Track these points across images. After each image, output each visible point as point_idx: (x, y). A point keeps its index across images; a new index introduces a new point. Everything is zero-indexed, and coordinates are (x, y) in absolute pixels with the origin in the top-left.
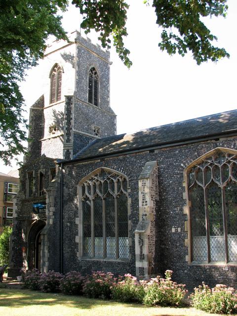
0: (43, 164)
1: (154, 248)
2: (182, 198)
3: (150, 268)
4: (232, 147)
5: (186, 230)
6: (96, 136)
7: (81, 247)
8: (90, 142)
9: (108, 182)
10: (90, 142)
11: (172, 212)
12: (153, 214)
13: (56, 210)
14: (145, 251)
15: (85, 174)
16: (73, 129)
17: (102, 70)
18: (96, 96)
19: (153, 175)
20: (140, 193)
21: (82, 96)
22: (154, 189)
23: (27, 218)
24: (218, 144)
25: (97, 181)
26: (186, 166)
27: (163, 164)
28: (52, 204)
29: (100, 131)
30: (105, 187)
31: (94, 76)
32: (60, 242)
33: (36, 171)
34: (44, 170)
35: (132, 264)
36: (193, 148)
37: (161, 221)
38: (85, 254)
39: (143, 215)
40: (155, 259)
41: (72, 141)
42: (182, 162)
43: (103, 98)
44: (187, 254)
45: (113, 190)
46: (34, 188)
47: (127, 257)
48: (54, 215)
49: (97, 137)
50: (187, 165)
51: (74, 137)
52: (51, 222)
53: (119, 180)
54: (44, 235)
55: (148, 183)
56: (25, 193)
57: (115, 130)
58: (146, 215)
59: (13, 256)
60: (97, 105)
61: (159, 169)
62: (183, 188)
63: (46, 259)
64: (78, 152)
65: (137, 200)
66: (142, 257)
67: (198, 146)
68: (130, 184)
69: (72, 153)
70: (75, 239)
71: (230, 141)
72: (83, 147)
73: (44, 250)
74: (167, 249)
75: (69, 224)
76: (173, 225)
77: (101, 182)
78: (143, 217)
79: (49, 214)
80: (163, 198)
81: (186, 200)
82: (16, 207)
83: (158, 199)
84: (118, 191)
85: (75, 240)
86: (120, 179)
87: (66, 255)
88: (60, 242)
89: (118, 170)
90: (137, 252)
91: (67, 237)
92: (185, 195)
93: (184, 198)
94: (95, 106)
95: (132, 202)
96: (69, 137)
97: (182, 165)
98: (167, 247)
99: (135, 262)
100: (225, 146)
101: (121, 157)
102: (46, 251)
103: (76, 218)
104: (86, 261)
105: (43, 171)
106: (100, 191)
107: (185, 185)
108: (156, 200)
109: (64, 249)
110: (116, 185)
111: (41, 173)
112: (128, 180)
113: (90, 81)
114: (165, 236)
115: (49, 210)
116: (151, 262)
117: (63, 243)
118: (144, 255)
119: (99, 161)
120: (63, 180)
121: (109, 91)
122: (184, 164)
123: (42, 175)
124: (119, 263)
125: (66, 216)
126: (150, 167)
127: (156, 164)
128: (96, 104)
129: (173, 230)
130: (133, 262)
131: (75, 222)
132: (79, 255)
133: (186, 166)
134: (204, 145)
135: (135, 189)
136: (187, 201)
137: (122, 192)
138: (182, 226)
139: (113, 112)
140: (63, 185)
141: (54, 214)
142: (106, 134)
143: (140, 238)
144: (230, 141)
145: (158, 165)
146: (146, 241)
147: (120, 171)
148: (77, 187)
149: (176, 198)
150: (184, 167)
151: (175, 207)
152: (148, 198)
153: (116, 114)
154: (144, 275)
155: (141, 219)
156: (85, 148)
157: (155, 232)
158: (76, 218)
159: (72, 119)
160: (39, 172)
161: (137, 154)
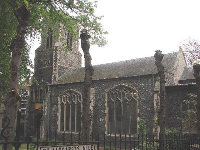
4: (127, 84)
44: (106, 131)
45: (75, 100)
52: (46, 114)
92: (106, 105)
93: (105, 106)
97: (105, 91)
106: (70, 101)
107: (106, 100)
110: (76, 98)
122: (106, 90)
129: (100, 120)
136: (107, 107)
137: (79, 102)
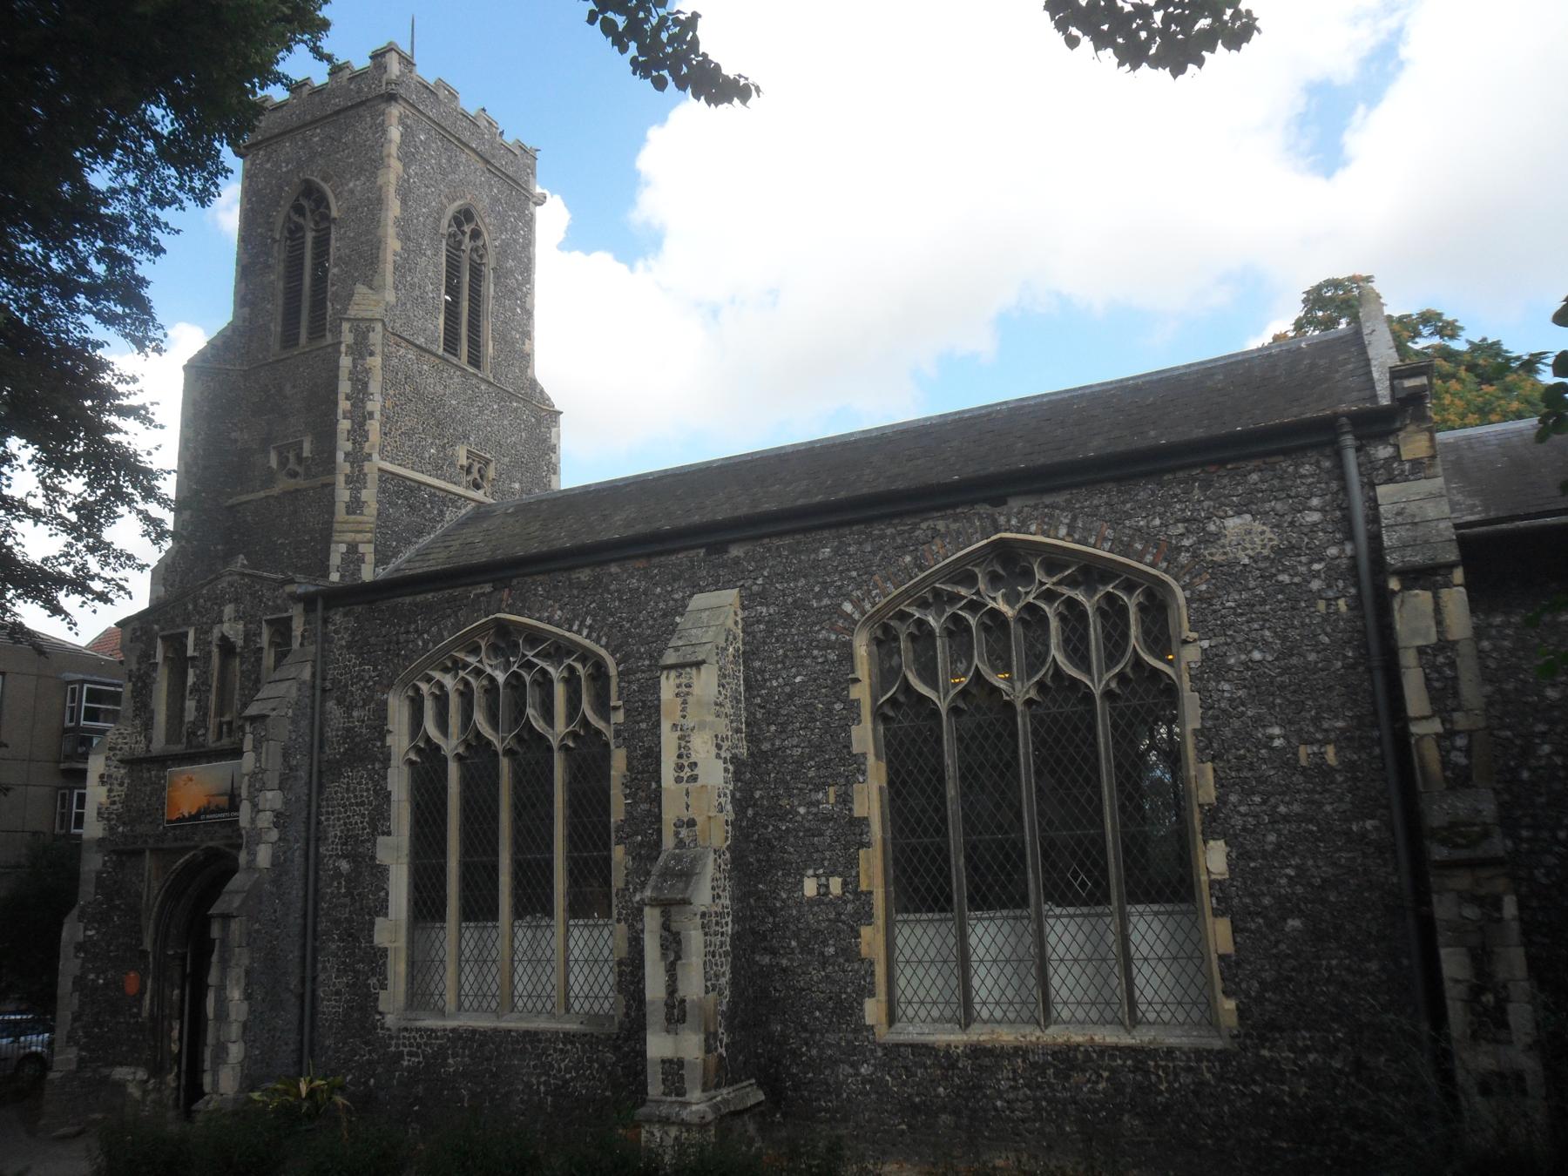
0: (236, 600)
1: (727, 969)
2: (848, 746)
3: (712, 1059)
4: (1063, 531)
5: (863, 887)
6: (472, 494)
7: (398, 969)
8: (450, 516)
9: (528, 679)
10: (450, 516)
11: (802, 810)
12: (722, 817)
13: (286, 802)
14: (693, 986)
15: (426, 643)
16: (375, 457)
17: (504, 224)
18: (474, 328)
19: (726, 649)
20: (666, 726)
21: (418, 324)
22: (728, 709)
23: (151, 841)
24: (1002, 520)
25: (478, 672)
26: (863, 613)
27: (761, 604)
28: (273, 779)
29: (491, 473)
30: (508, 702)
31: (467, 244)
32: (304, 946)
33: (203, 632)
34: (241, 626)
35: (626, 1040)
36: (893, 538)
37: (758, 855)
38: (419, 996)
39: (679, 824)
40: (731, 1017)
41: (372, 509)
42: (847, 596)
43: (502, 339)
44: (872, 994)
45: (548, 714)
46: (190, 704)
47: (607, 1006)
48: (276, 825)
49: (478, 495)
50: (868, 606)
51: (382, 490)
52: (264, 856)
53: (571, 669)
54: (226, 917)
55: (706, 683)
56: (148, 726)
57: (554, 470)
58: (691, 823)
59: (75, 1019)
60: (478, 367)
61: (747, 625)
62: (853, 706)
63: (235, 1030)
64: (395, 555)
65: (653, 757)
66: (676, 1013)
67: (915, 527)
68: (621, 690)
69: (370, 558)
70: (371, 929)
71: (1053, 506)
72: (420, 534)
73: (221, 988)
74: (784, 970)
75: (344, 865)
76: (807, 867)
77: (492, 679)
78: (677, 834)
79: (253, 821)
80: (766, 746)
81: (864, 755)
82: (103, 790)
83: (743, 751)
84: (570, 718)
85: (371, 936)
86: (578, 666)
87: (329, 1007)
88: (304, 946)
89: (570, 630)
90: (654, 986)
91: (337, 922)
92: (864, 736)
93: (856, 749)
94: (471, 370)
95: (630, 767)
96: (358, 490)
97: (848, 607)
98: (784, 962)
99: (643, 1028)
100: (1033, 528)
101: (584, 575)
102: (235, 994)
103: (381, 839)
104: (418, 1030)
105: (232, 629)
106: (494, 724)
107: (861, 692)
108: (734, 759)
109: (322, 977)
110: (560, 691)
111: (224, 638)
112: (613, 671)
113: (453, 268)
114: (772, 912)
115: (255, 805)
116: (716, 1034)
117: (315, 950)
118: (683, 1001)
119: (488, 588)
120: (323, 671)
121: (529, 314)
122: (857, 604)
123: (227, 647)
124: (569, 1038)
125: (335, 832)
126: (715, 613)
127: (738, 604)
128: (475, 361)
129: (810, 888)
130: (635, 1029)
131: (373, 858)
132: (392, 1003)
133: (863, 613)
134: (941, 525)
135: (646, 710)
136: (871, 759)
137: (585, 723)
138: (848, 868)
139: (545, 399)
140: (324, 691)
141: (280, 819)
142: (517, 486)
143: (666, 927)
144: (1053, 506)
145: (744, 608)
146: (695, 940)
147: (579, 632)
148: (385, 703)
149: (820, 749)
150: (856, 616)
151: (818, 788)
152: (702, 747)
153: (557, 408)
154: (683, 1094)
155: (668, 841)
156: (426, 539)
157: (732, 899)
158: (381, 839)
159: (371, 414)
160: (216, 632)
161: (655, 561)
